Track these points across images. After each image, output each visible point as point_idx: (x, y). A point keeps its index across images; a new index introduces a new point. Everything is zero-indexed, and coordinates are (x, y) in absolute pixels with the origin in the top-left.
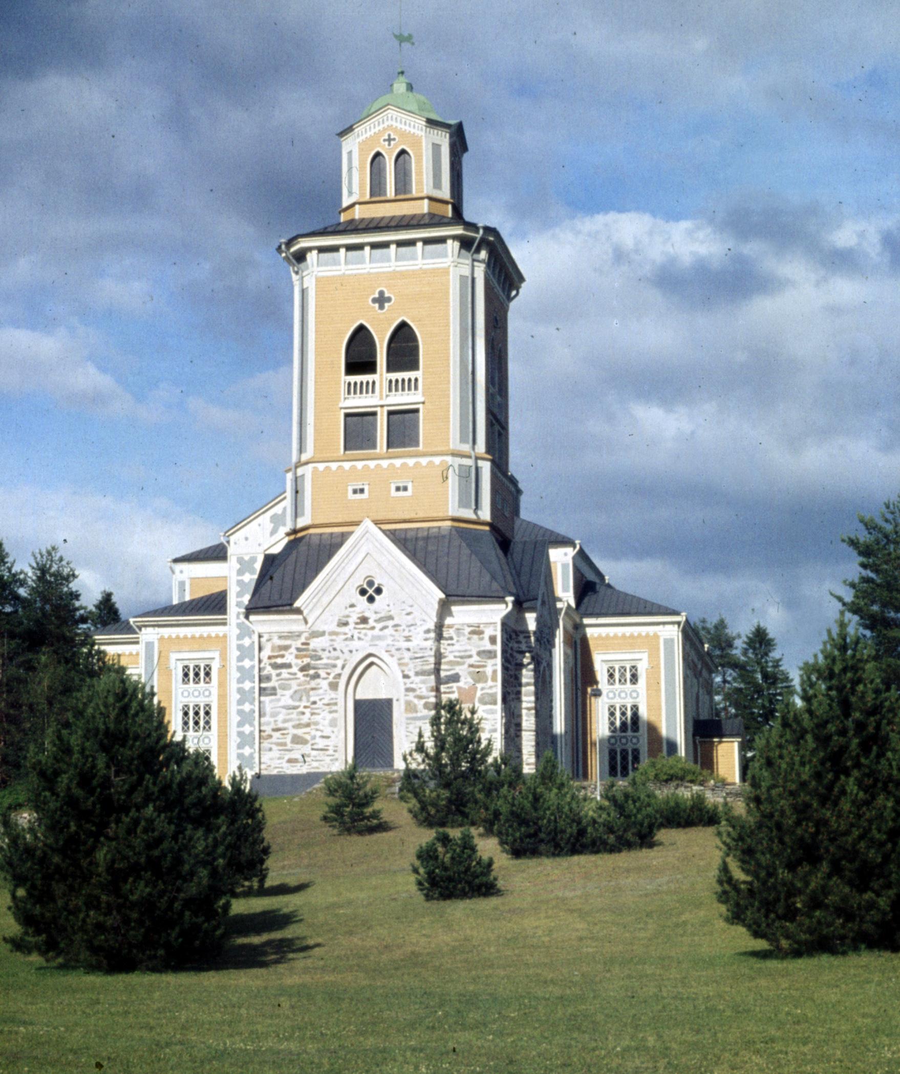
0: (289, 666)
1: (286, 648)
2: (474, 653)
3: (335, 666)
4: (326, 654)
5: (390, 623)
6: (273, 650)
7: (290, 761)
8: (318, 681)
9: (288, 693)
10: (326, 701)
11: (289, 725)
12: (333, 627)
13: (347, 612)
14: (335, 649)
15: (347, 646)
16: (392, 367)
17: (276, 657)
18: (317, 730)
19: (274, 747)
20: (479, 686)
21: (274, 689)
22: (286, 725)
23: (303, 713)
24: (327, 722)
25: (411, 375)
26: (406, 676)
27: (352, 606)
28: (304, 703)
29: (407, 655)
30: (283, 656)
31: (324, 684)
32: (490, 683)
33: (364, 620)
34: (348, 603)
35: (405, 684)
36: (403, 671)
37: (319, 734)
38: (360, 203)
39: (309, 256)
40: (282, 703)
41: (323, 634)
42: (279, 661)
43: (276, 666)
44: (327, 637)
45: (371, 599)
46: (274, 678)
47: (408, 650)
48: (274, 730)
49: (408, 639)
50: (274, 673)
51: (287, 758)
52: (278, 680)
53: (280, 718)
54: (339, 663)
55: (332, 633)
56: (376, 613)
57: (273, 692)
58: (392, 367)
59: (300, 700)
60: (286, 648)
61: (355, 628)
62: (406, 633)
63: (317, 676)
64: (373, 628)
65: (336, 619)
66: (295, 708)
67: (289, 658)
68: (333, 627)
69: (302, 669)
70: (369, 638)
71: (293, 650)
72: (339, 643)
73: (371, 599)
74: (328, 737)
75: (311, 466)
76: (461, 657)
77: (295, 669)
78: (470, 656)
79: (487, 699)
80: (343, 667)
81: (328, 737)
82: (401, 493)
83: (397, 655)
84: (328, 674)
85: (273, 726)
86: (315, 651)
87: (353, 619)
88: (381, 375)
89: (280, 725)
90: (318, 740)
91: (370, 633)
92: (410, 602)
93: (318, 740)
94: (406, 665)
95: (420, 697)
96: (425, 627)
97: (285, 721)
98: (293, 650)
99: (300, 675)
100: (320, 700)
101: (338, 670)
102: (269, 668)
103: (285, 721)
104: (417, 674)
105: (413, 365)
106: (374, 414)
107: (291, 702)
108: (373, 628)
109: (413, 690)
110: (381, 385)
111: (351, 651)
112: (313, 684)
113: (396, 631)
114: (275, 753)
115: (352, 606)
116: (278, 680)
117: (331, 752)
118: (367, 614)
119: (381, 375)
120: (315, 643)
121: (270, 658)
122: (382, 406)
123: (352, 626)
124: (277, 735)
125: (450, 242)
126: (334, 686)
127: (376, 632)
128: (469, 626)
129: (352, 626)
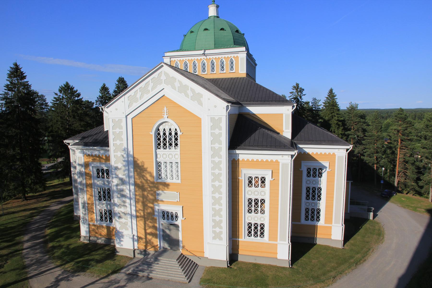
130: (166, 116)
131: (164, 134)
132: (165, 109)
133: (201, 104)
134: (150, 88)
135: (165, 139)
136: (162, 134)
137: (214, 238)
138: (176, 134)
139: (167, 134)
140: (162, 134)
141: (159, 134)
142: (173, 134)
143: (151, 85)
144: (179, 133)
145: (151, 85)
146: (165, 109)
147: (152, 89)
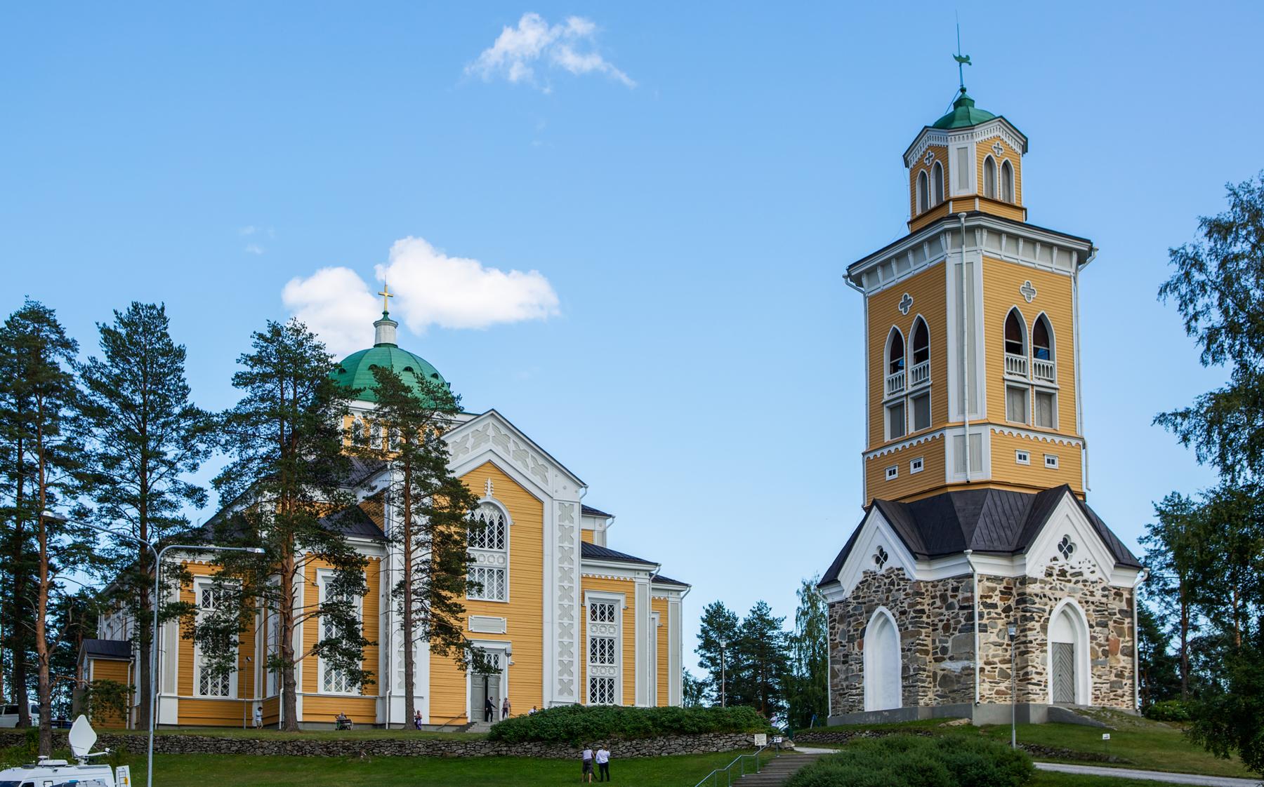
0: (994, 606)
1: (993, 590)
3: (1044, 611)
4: (1037, 600)
5: (1080, 578)
7: (998, 693)
9: (996, 631)
11: (996, 660)
12: (1041, 576)
13: (1051, 564)
17: (987, 597)
26: (1091, 626)
27: (1055, 559)
29: (1092, 607)
30: (991, 597)
31: (1037, 626)
33: (1063, 573)
38: (981, 198)
40: (991, 640)
41: (1035, 581)
42: (989, 601)
43: (986, 605)
44: (1038, 585)
48: (986, 663)
50: (986, 611)
53: (991, 652)
54: (1047, 608)
55: (1042, 581)
57: (984, 629)
58: (1036, 353)
60: (993, 590)
63: (1032, 619)
66: (1001, 645)
67: (996, 599)
68: (1041, 576)
69: (1004, 611)
70: (1066, 590)
71: (997, 592)
75: (990, 427)
77: (999, 610)
82: (1051, 466)
87: (1057, 568)
90: (1034, 676)
91: (1068, 585)
92: (1093, 562)
93: (1034, 676)
95: (1100, 645)
96: (1104, 584)
97: (994, 656)
98: (997, 592)
99: (1003, 615)
103: (994, 656)
104: (1098, 625)
105: (1048, 356)
107: (997, 640)
108: (1069, 581)
112: (1030, 625)
114: (987, 685)
115: (1055, 559)
118: (1067, 568)
120: (1032, 589)
123: (1055, 577)
124: (988, 668)
126: (1044, 629)
127: (1071, 585)
129: (1055, 577)
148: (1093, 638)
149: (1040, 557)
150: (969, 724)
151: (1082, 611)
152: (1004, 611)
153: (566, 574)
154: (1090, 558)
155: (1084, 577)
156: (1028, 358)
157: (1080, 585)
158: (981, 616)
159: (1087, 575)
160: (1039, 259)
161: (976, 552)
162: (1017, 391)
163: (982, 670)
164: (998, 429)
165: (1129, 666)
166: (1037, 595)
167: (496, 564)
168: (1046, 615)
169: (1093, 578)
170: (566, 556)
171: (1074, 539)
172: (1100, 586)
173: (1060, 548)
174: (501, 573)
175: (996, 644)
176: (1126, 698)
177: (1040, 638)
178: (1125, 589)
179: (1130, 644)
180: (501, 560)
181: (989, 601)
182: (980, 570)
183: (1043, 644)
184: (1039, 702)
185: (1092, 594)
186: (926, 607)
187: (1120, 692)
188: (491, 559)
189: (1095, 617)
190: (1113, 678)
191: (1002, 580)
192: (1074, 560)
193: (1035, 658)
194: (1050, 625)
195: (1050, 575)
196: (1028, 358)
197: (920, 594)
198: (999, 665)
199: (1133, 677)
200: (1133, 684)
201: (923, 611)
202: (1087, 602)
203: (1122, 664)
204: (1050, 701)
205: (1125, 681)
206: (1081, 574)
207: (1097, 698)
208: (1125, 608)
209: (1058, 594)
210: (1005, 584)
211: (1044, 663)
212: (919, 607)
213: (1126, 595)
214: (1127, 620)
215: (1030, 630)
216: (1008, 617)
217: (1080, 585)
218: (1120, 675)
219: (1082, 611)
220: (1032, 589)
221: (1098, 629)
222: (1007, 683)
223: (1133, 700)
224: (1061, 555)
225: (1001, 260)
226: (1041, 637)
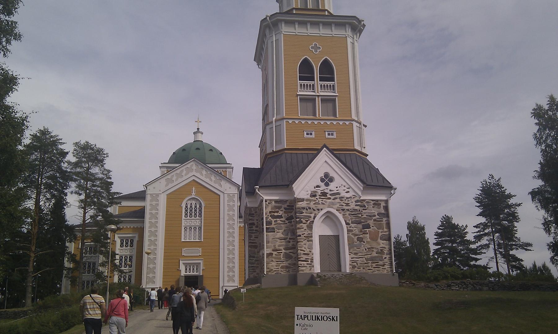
2: (376, 214)
4: (304, 211)
6: (271, 209)
8: (302, 224)
10: (304, 235)
11: (281, 248)
12: (309, 197)
13: (314, 190)
14: (310, 208)
15: (316, 207)
16: (321, 79)
18: (301, 250)
19: (274, 260)
20: (380, 231)
21: (273, 228)
22: (280, 248)
23: (290, 242)
24: (306, 246)
25: (331, 83)
27: (318, 186)
28: (289, 236)
29: (348, 213)
30: (278, 212)
31: (305, 226)
32: (385, 230)
33: (324, 194)
34: (315, 185)
35: (347, 227)
36: (345, 221)
37: (302, 252)
38: (296, 9)
39: (279, 24)
41: (302, 200)
42: (276, 214)
43: (273, 217)
45: (327, 185)
46: (273, 223)
47: (348, 210)
48: (273, 250)
49: (347, 205)
50: (273, 220)
51: (281, 265)
52: (275, 224)
54: (312, 215)
55: (307, 200)
56: (330, 191)
59: (287, 235)
61: (320, 198)
62: (346, 202)
63: (302, 222)
64: (330, 198)
65: (310, 192)
68: (309, 197)
69: (287, 219)
71: (282, 209)
72: (312, 205)
73: (327, 185)
74: (308, 254)
76: (370, 216)
78: (375, 216)
79: (384, 238)
80: (314, 219)
81: (308, 254)
83: (343, 213)
84: (307, 221)
85: (273, 248)
86: (299, 208)
87: (319, 192)
88: (317, 82)
89: (277, 248)
90: (302, 256)
93: (302, 256)
94: (346, 217)
95: (355, 235)
96: (356, 199)
98: (282, 209)
99: (287, 222)
100: (303, 234)
101: (312, 219)
102: (270, 218)
103: (279, 246)
106: (315, 100)
107: (282, 236)
108: (330, 198)
109: (351, 231)
110: (318, 86)
111: (318, 210)
112: (298, 226)
113: (342, 200)
114: (274, 264)
115: (318, 186)
116: (275, 224)
117: (309, 262)
119: (317, 82)
120: (300, 204)
121: (270, 212)
122: (318, 96)
123: (318, 197)
124: (275, 253)
125: (347, 26)
126: (310, 227)
128: (373, 200)
130: (194, 193)
131: (191, 207)
132: (194, 189)
133: (221, 186)
134: (183, 174)
135: (191, 211)
136: (189, 207)
137: (228, 281)
138: (200, 206)
139: (193, 207)
140: (189, 207)
141: (187, 207)
142: (198, 206)
143: (185, 172)
144: (203, 206)
145: (185, 172)
146: (194, 189)
147: (186, 175)
148: (348, 231)
149: (304, 186)
150: (259, 287)
151: (340, 216)
152: (287, 219)
153: (231, 226)
154: (344, 184)
155: (340, 196)
156: (317, 82)
157: (338, 200)
158: (269, 223)
159: (343, 194)
160: (336, 32)
161: (261, 187)
162: (309, 100)
163: (270, 255)
164: (290, 121)
165: (387, 247)
166: (304, 208)
167: (198, 224)
168: (312, 219)
169: (348, 195)
170: (231, 218)
171: (332, 174)
172: (353, 200)
173: (322, 180)
174: (200, 228)
175: (281, 239)
176: (386, 267)
177: (306, 233)
178: (381, 200)
179: (387, 233)
180: (200, 223)
181: (276, 214)
182: (266, 198)
183: (309, 238)
184: (307, 271)
185: (347, 205)
186: (255, 222)
187: (381, 263)
188: (195, 223)
189: (350, 219)
190: (374, 254)
191: (286, 201)
192: (332, 186)
193: (303, 245)
194: (315, 226)
195: (315, 196)
196: (317, 82)
197: (251, 215)
198: (283, 251)
199: (391, 253)
200: (391, 258)
201: (253, 224)
202: (343, 210)
203: (382, 245)
204: (317, 269)
205: (384, 256)
206: (338, 194)
207: (354, 267)
208: (383, 212)
209: (320, 207)
210: (288, 204)
211: (311, 247)
212: (251, 222)
213: (383, 204)
214: (385, 219)
215: (299, 228)
216: (291, 222)
217: (338, 200)
218: (381, 252)
219: (340, 216)
220: (300, 204)
221: (353, 225)
222: (289, 262)
223: (391, 267)
224: (322, 184)
225: (296, 35)
226: (306, 233)
